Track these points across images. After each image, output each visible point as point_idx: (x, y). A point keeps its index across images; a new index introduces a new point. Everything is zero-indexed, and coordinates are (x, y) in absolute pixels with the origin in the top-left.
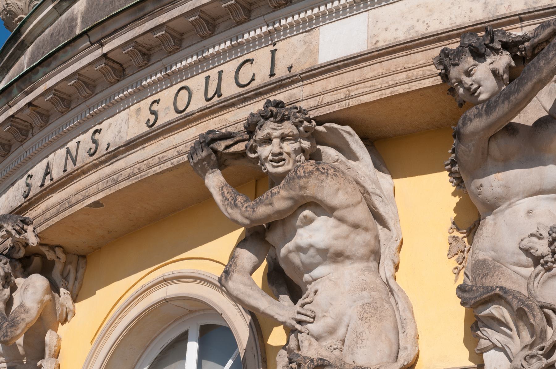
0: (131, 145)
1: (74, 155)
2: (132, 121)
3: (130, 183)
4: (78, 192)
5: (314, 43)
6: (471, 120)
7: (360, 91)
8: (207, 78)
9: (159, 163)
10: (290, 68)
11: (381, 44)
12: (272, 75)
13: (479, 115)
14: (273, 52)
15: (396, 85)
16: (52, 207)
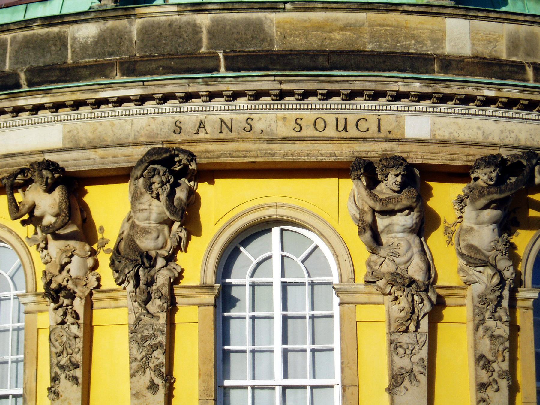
0: (286, 139)
1: (230, 126)
2: (280, 123)
3: (285, 160)
4: (238, 151)
5: (402, 123)
6: (492, 194)
7: (429, 157)
8: (337, 119)
9: (308, 156)
10: (390, 132)
11: (438, 137)
12: (379, 131)
13: (496, 193)
14: (379, 120)
15: (446, 160)
16: (213, 151)
